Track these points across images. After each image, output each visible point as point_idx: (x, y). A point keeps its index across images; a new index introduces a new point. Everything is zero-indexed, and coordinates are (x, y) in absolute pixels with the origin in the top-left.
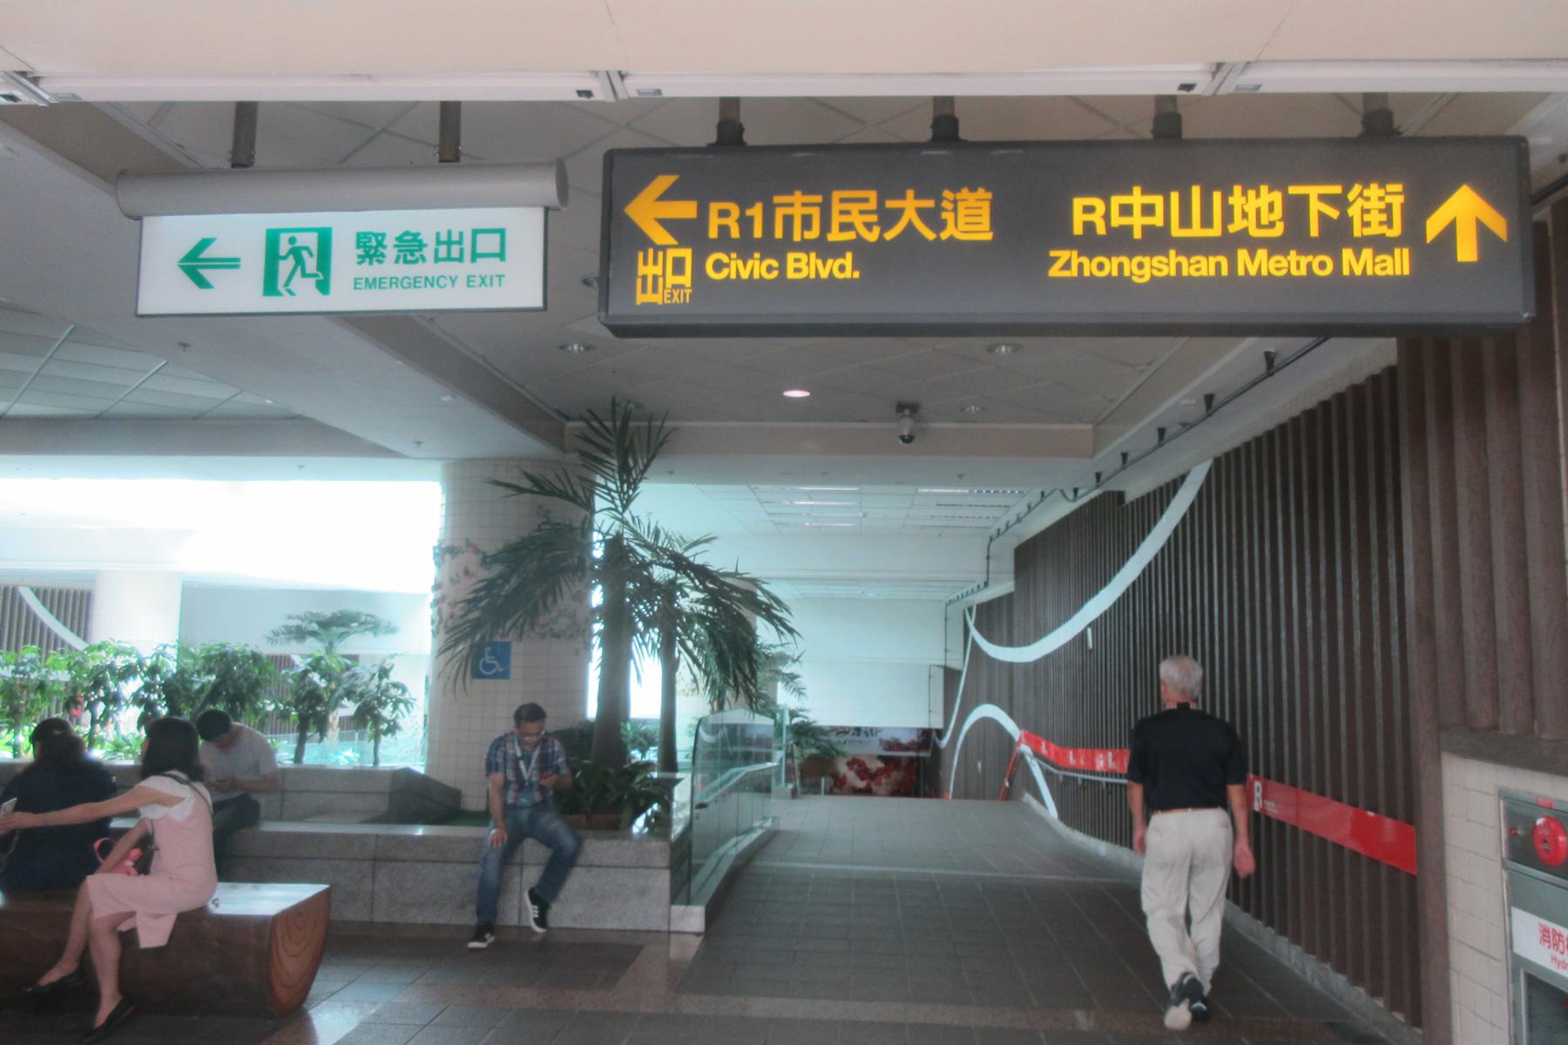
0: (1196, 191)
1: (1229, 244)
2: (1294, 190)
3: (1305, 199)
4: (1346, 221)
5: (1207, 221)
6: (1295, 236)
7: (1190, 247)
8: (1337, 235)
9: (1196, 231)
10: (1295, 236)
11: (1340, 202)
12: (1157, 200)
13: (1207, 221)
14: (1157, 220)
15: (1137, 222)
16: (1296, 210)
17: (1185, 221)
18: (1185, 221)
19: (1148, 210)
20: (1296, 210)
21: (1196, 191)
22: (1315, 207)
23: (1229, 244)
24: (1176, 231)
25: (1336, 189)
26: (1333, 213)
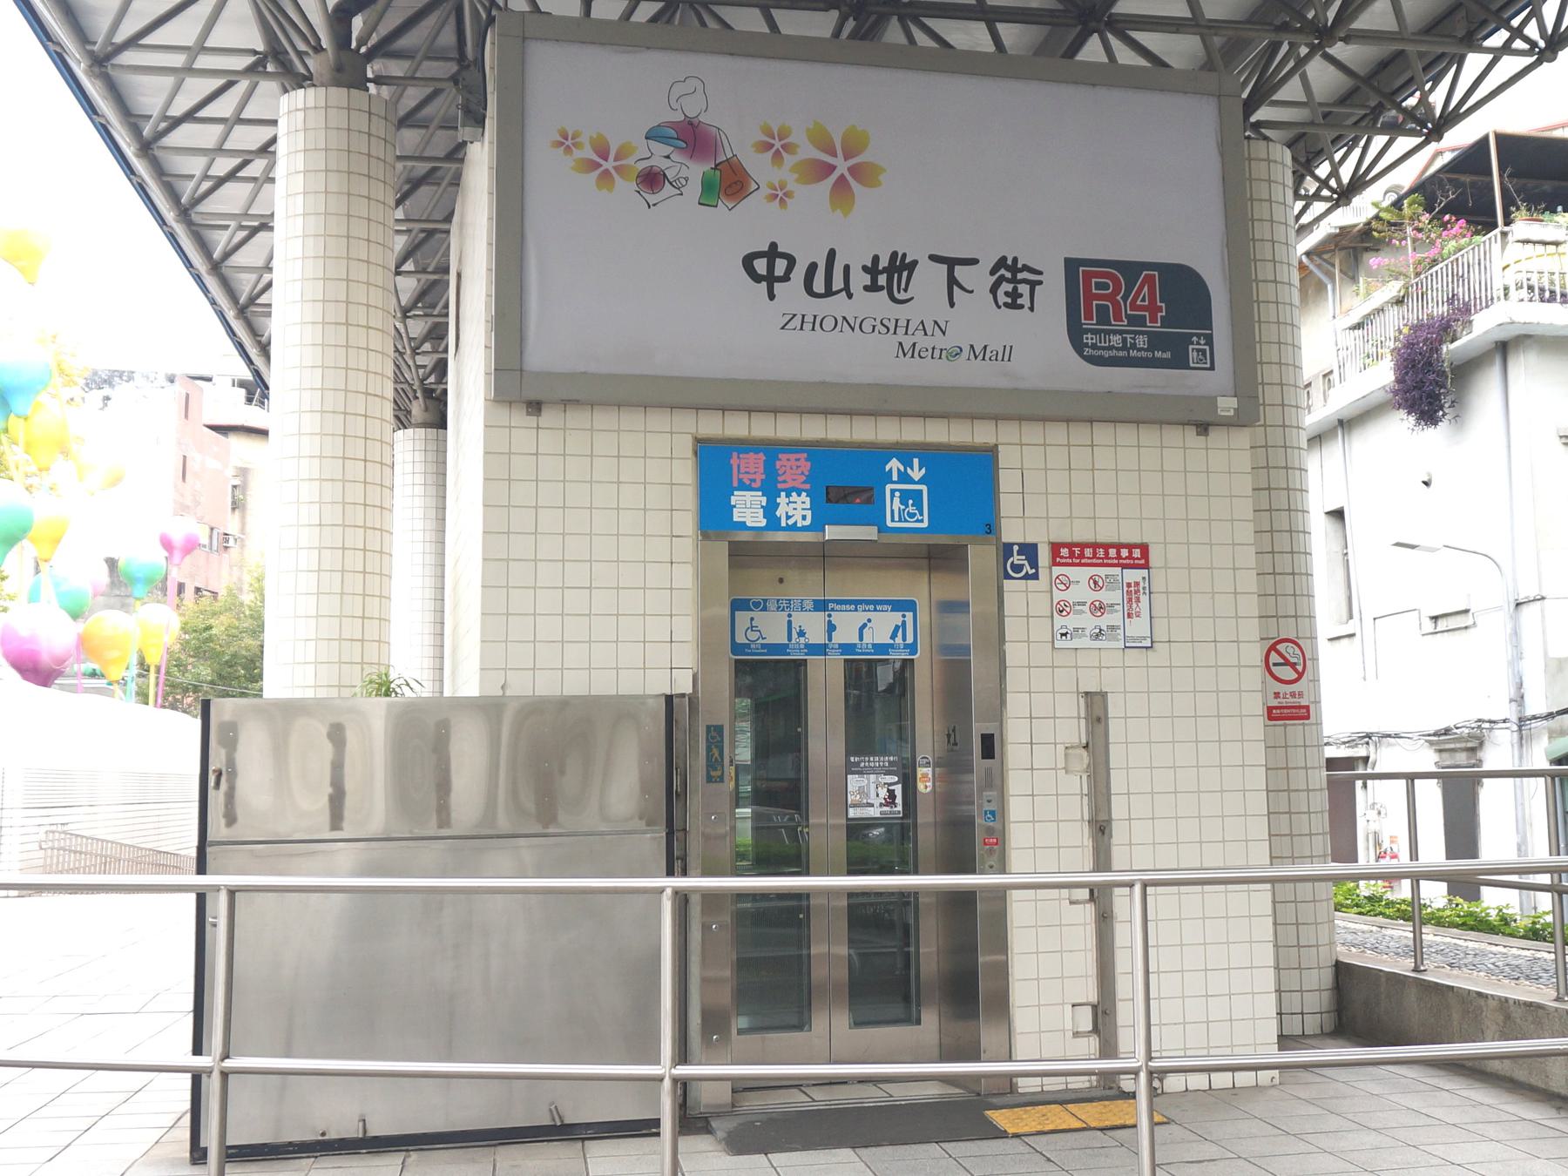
0: (1103, 335)
1: (1111, 348)
2: (1124, 335)
3: (1126, 338)
4: (1135, 343)
5: (1105, 343)
6: (1124, 348)
7: (1104, 348)
8: (1134, 346)
9: (1103, 344)
10: (1124, 348)
11: (1134, 339)
12: (1094, 337)
13: (1105, 343)
14: (1094, 341)
15: (1090, 341)
16: (1124, 340)
17: (1100, 342)
18: (1100, 342)
19: (1092, 339)
20: (1124, 340)
21: (1103, 335)
22: (1129, 340)
23: (1111, 348)
24: (1099, 344)
25: (1133, 336)
26: (1133, 341)
